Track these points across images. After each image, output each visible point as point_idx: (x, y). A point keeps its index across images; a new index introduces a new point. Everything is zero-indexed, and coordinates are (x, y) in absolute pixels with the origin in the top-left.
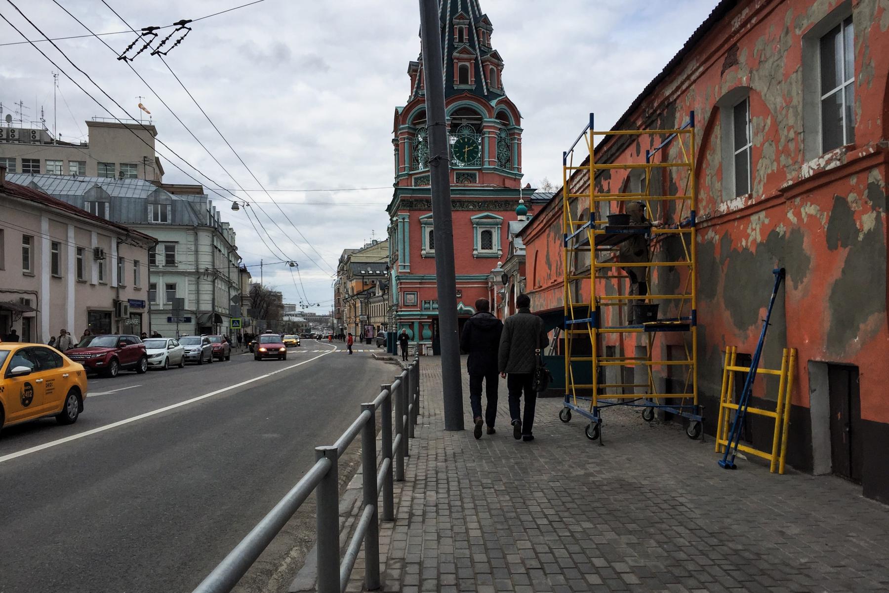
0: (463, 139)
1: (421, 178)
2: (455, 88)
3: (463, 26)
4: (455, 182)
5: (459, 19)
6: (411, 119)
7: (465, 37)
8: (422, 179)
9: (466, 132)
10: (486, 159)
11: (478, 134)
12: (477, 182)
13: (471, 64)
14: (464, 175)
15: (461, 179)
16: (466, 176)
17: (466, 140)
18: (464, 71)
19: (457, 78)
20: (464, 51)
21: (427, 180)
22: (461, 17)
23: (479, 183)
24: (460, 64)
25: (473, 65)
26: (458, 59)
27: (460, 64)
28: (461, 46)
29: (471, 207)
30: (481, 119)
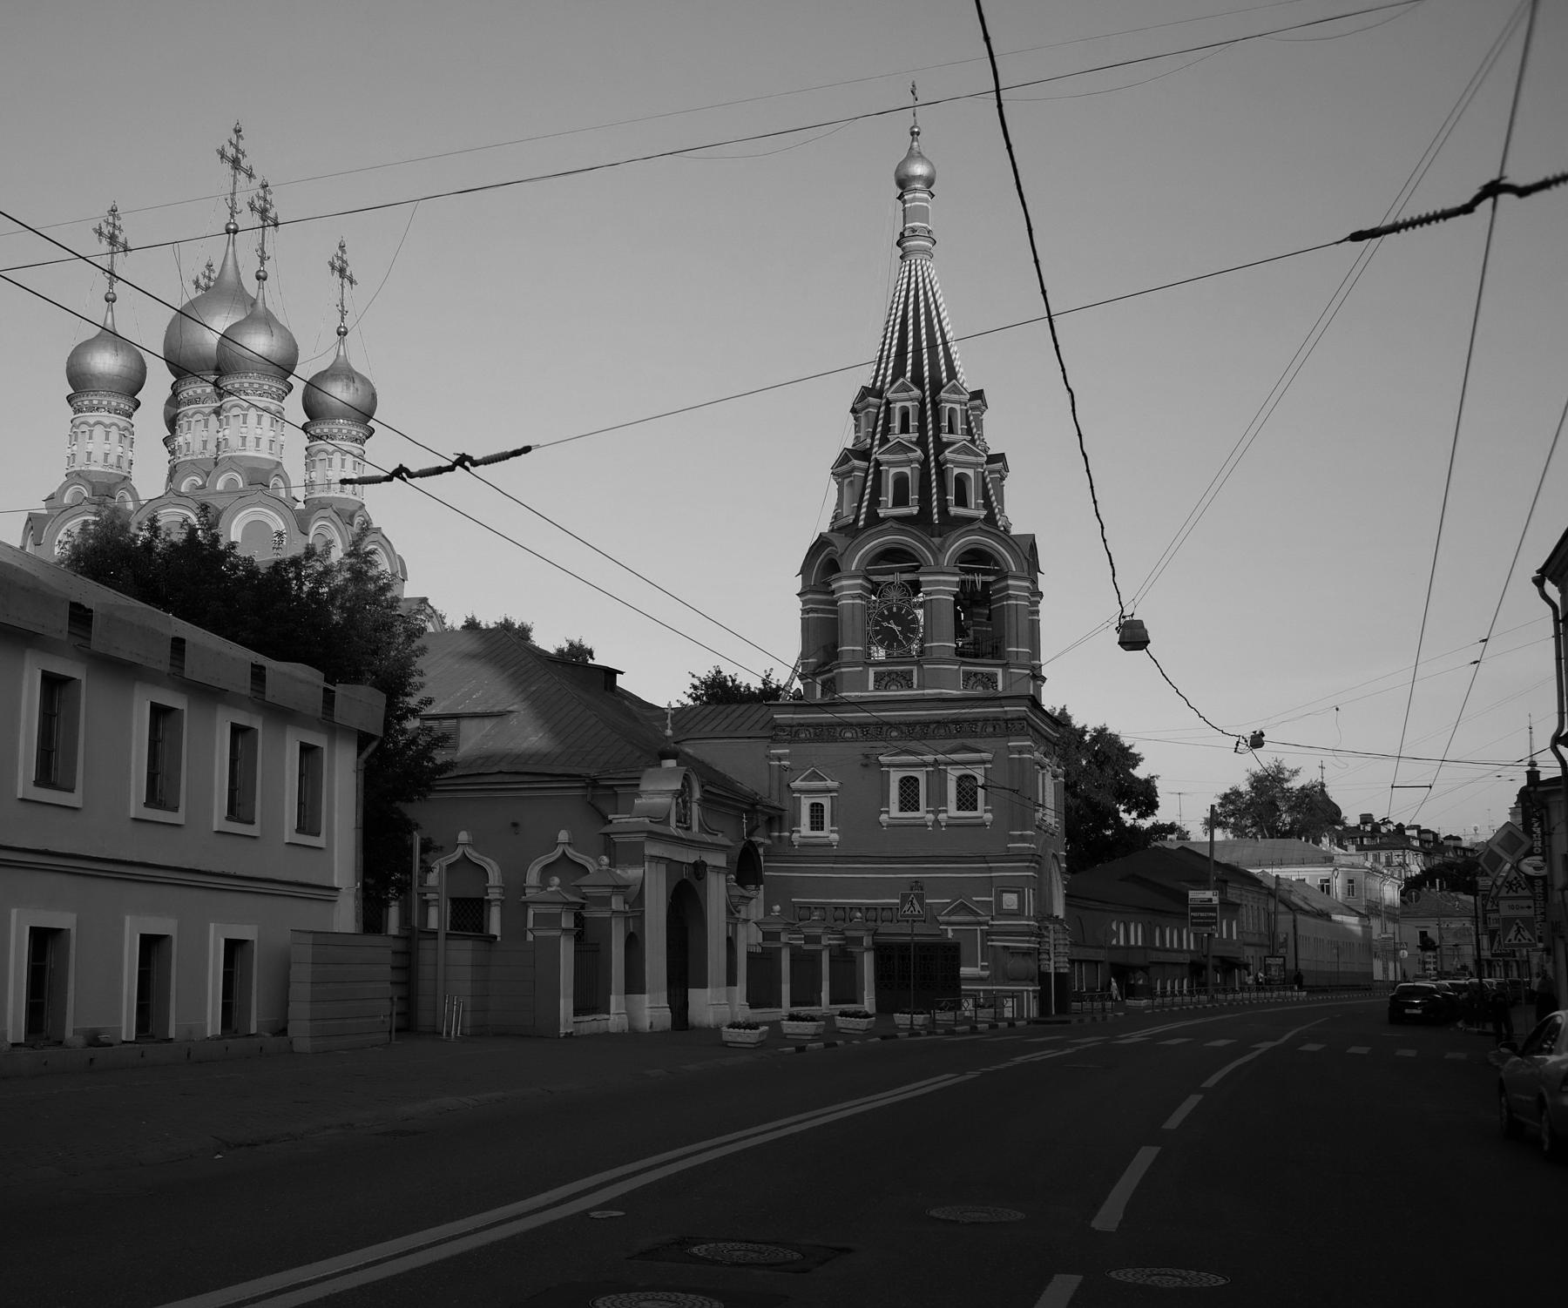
1: (890, 673)
2: (952, 513)
5: (950, 393)
6: (866, 563)
7: (960, 425)
8: (894, 676)
13: (976, 473)
14: (976, 674)
15: (971, 683)
18: (961, 481)
19: (951, 498)
20: (964, 450)
25: (980, 475)
26: (953, 462)
27: (957, 471)
30: (1003, 575)
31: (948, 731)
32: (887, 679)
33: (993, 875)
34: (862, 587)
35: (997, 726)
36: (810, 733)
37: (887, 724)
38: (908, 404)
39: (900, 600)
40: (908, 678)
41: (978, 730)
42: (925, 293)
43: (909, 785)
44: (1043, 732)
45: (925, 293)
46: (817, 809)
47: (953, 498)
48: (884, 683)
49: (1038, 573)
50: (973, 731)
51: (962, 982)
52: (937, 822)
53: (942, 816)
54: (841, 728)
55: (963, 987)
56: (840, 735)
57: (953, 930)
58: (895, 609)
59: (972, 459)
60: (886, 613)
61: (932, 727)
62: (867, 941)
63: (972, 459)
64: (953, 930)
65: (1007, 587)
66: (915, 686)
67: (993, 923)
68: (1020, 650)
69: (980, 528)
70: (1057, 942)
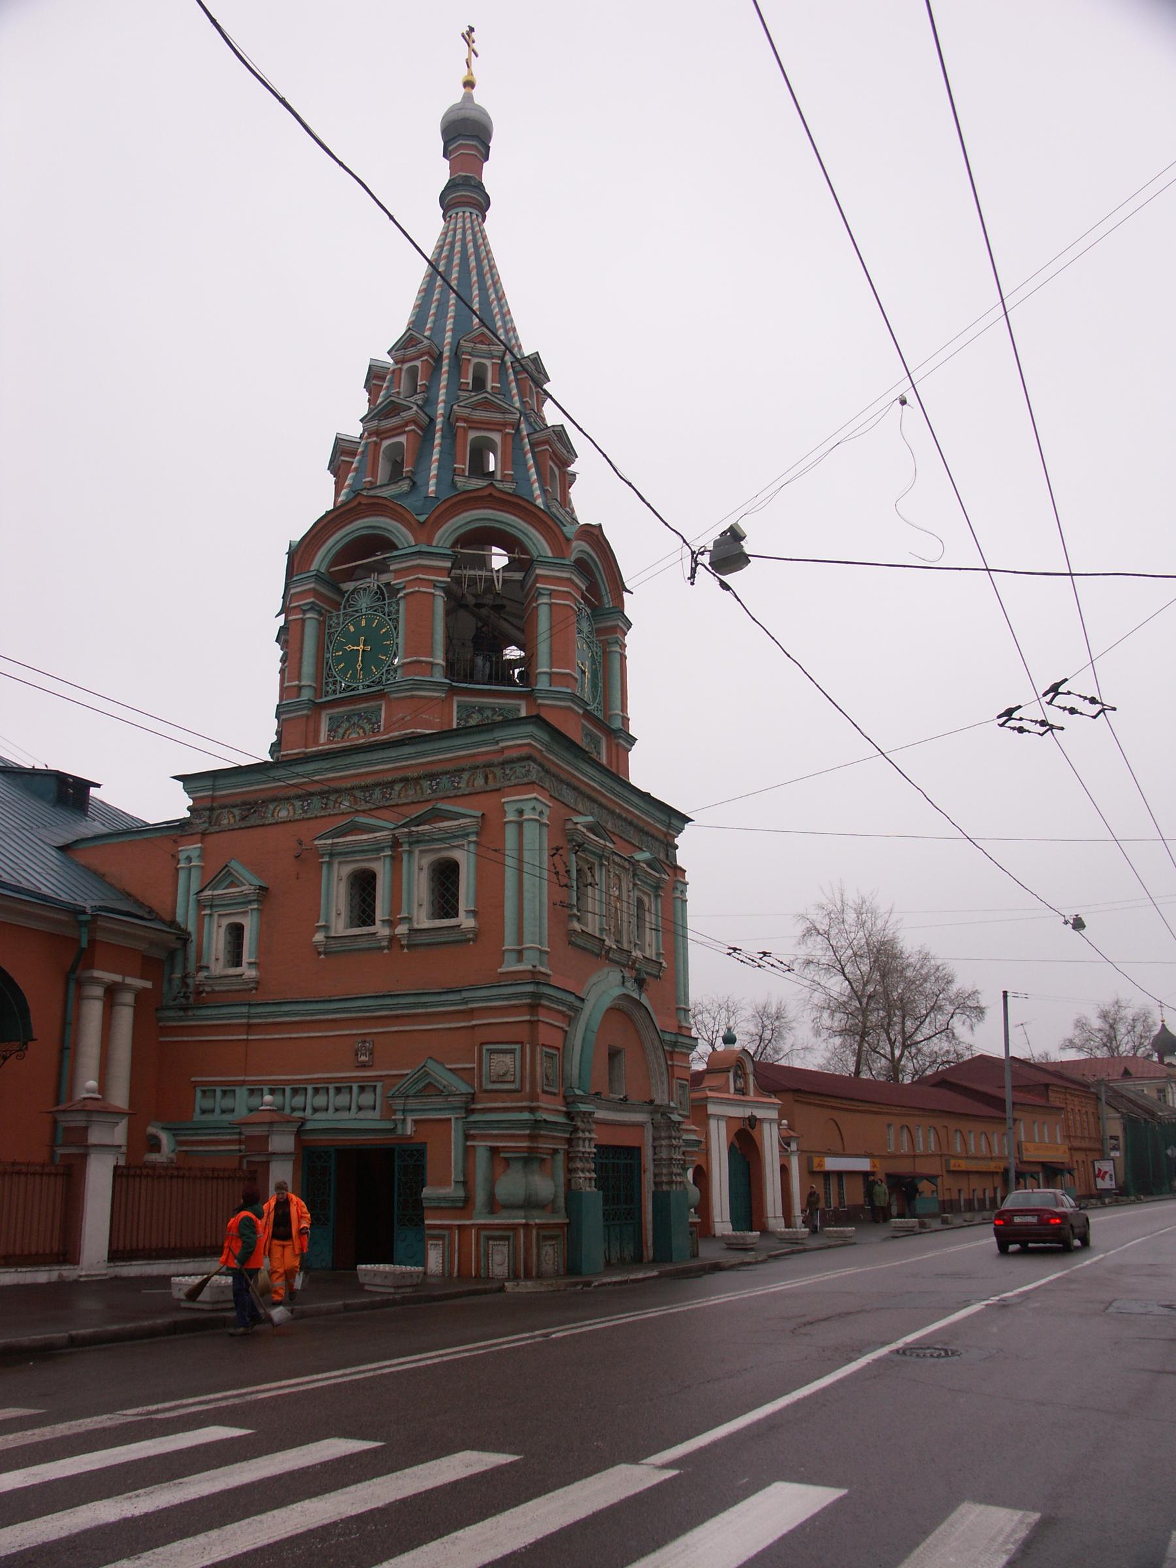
3: (488, 362)
8: (356, 719)
20: (486, 405)
21: (369, 720)
22: (482, 339)
24: (472, 435)
31: (419, 792)
32: (345, 725)
33: (474, 1023)
34: (314, 592)
35: (490, 776)
36: (234, 817)
37: (337, 791)
38: (418, 363)
39: (371, 608)
40: (374, 720)
41: (462, 785)
43: (364, 884)
44: (583, 788)
46: (236, 932)
48: (341, 731)
49: (625, 594)
50: (456, 788)
51: (427, 1213)
52: (393, 939)
53: (402, 929)
54: (276, 804)
55: (427, 1222)
56: (273, 816)
57: (415, 1122)
58: (363, 623)
59: (497, 416)
60: (352, 629)
61: (397, 787)
62: (283, 1142)
63: (497, 416)
64: (415, 1122)
65: (536, 581)
66: (382, 729)
67: (473, 1106)
68: (554, 670)
69: (491, 494)
70: (657, 1143)
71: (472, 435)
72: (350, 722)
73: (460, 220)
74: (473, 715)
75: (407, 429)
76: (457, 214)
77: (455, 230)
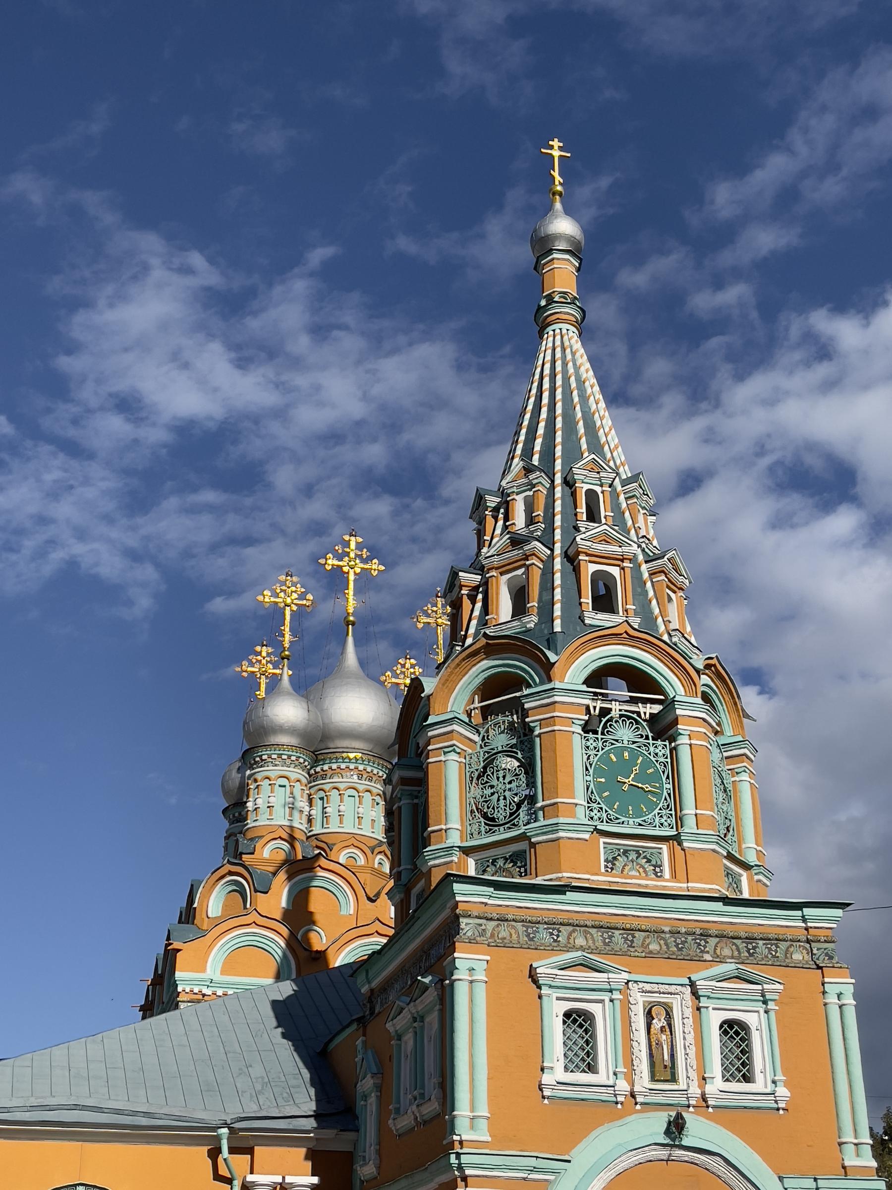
0: (619, 752)
3: (598, 489)
4: (603, 870)
9: (625, 734)
10: (689, 810)
11: (659, 742)
12: (667, 874)
15: (619, 864)
16: (633, 856)
17: (626, 754)
19: (587, 600)
20: (606, 539)
23: (674, 876)
24: (593, 568)
28: (596, 529)
29: (654, 947)
42: (565, 364)
45: (565, 364)
47: (590, 601)
71: (593, 568)
72: (495, 866)
73: (558, 338)
74: (618, 857)
75: (528, 563)
76: (554, 331)
77: (554, 349)
